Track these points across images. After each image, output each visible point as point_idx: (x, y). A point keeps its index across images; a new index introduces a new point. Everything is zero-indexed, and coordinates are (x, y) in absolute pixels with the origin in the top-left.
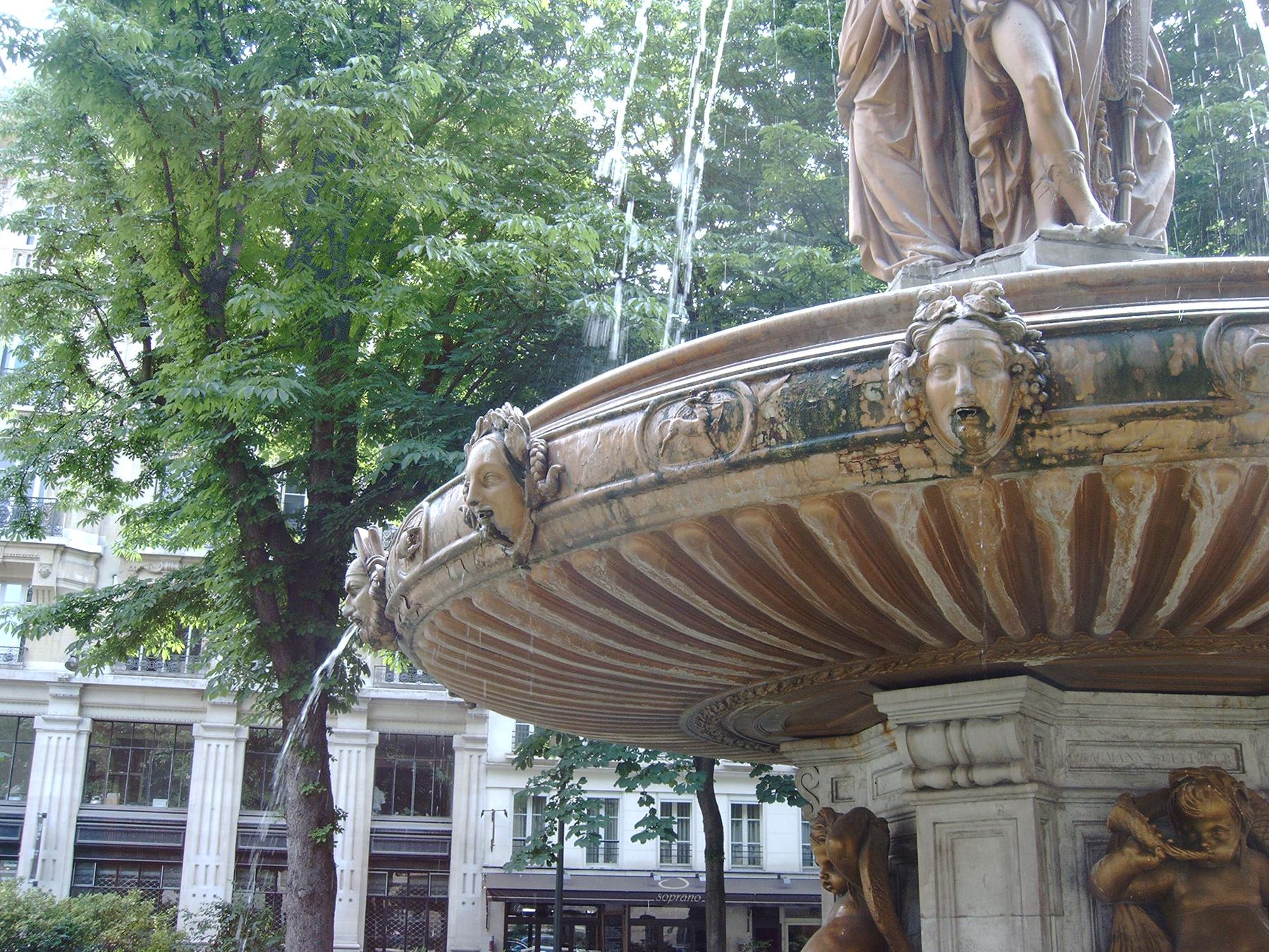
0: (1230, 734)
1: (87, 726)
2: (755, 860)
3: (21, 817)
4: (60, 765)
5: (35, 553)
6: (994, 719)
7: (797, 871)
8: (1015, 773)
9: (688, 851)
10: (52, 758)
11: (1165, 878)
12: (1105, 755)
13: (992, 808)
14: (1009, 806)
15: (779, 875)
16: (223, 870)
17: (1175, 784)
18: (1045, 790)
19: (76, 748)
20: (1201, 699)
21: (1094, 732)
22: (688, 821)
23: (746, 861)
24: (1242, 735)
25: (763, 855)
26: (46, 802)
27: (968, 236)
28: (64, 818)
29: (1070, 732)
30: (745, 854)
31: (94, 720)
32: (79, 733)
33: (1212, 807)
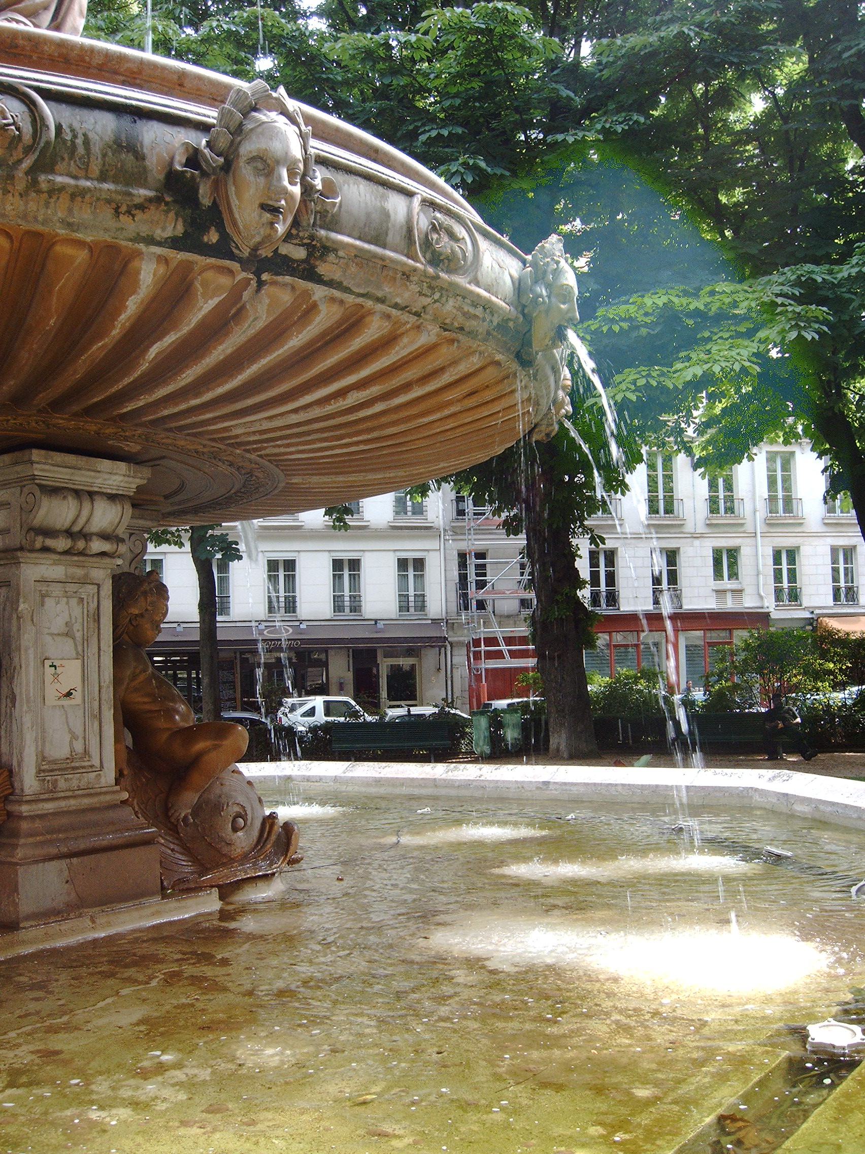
2: (356, 608)
7: (394, 617)
9: (294, 602)
15: (376, 621)
22: (294, 576)
23: (347, 610)
25: (363, 604)
30: (347, 604)
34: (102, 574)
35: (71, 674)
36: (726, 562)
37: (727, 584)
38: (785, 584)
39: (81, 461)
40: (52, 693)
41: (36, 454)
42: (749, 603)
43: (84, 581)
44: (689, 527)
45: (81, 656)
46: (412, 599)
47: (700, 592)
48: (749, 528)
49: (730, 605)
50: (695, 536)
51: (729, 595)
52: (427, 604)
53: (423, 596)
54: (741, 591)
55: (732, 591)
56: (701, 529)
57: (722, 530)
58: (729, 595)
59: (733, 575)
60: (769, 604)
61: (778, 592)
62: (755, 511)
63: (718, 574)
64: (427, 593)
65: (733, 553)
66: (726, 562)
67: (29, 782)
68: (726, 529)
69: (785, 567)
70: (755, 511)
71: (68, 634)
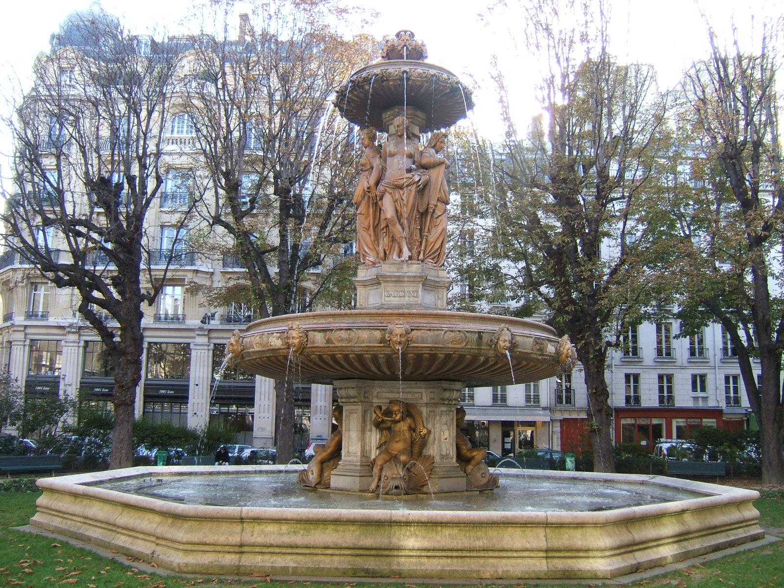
0: (419, 390)
1: (212, 347)
3: (188, 386)
4: (202, 364)
5: (185, 273)
6: (353, 388)
8: (356, 400)
10: (198, 361)
11: (389, 424)
12: (387, 395)
13: (355, 407)
14: (358, 407)
16: (271, 406)
17: (390, 403)
18: (364, 404)
19: (208, 357)
20: (410, 382)
21: (384, 390)
24: (423, 391)
26: (197, 379)
27: (382, 254)
28: (205, 386)
29: (378, 390)
31: (215, 344)
32: (209, 350)
33: (395, 408)
34: (454, 409)
35: (446, 434)
36: (699, 382)
37: (700, 394)
38: (732, 395)
39: (452, 383)
40: (443, 438)
41: (443, 382)
42: (711, 404)
43: (451, 411)
44: (679, 363)
45: (448, 429)
46: (532, 397)
47: (684, 397)
48: (712, 364)
49: (701, 404)
50: (682, 368)
51: (700, 400)
52: (540, 400)
53: (538, 396)
54: (707, 398)
55: (702, 397)
56: (685, 364)
57: (697, 365)
58: (700, 400)
59: (703, 389)
60: (723, 405)
61: (728, 398)
62: (715, 355)
63: (694, 388)
64: (540, 394)
65: (703, 377)
66: (699, 382)
67: (437, 459)
68: (699, 364)
69: (731, 385)
70: (715, 355)
71: (447, 424)
